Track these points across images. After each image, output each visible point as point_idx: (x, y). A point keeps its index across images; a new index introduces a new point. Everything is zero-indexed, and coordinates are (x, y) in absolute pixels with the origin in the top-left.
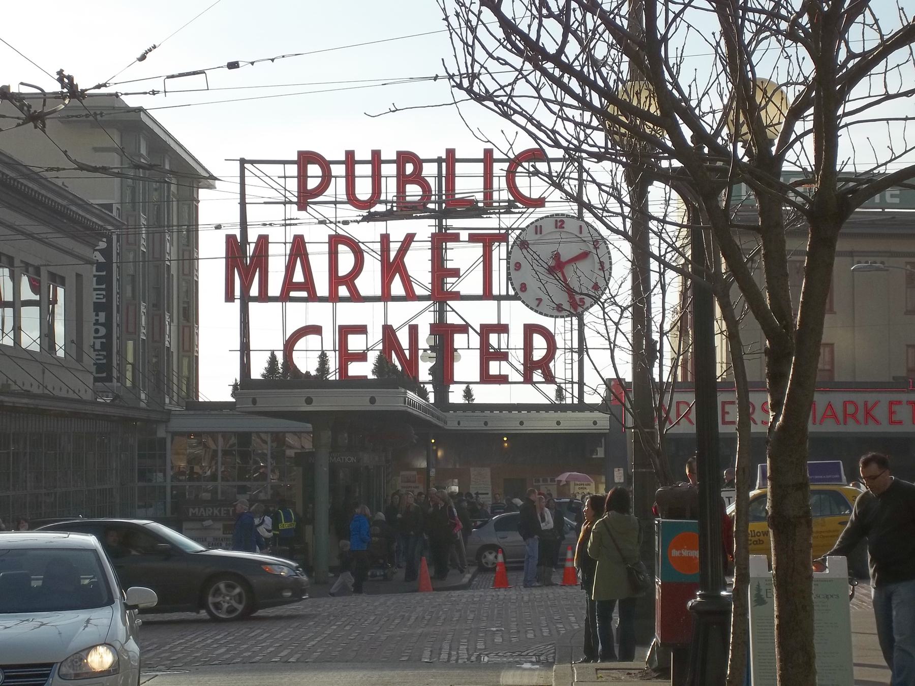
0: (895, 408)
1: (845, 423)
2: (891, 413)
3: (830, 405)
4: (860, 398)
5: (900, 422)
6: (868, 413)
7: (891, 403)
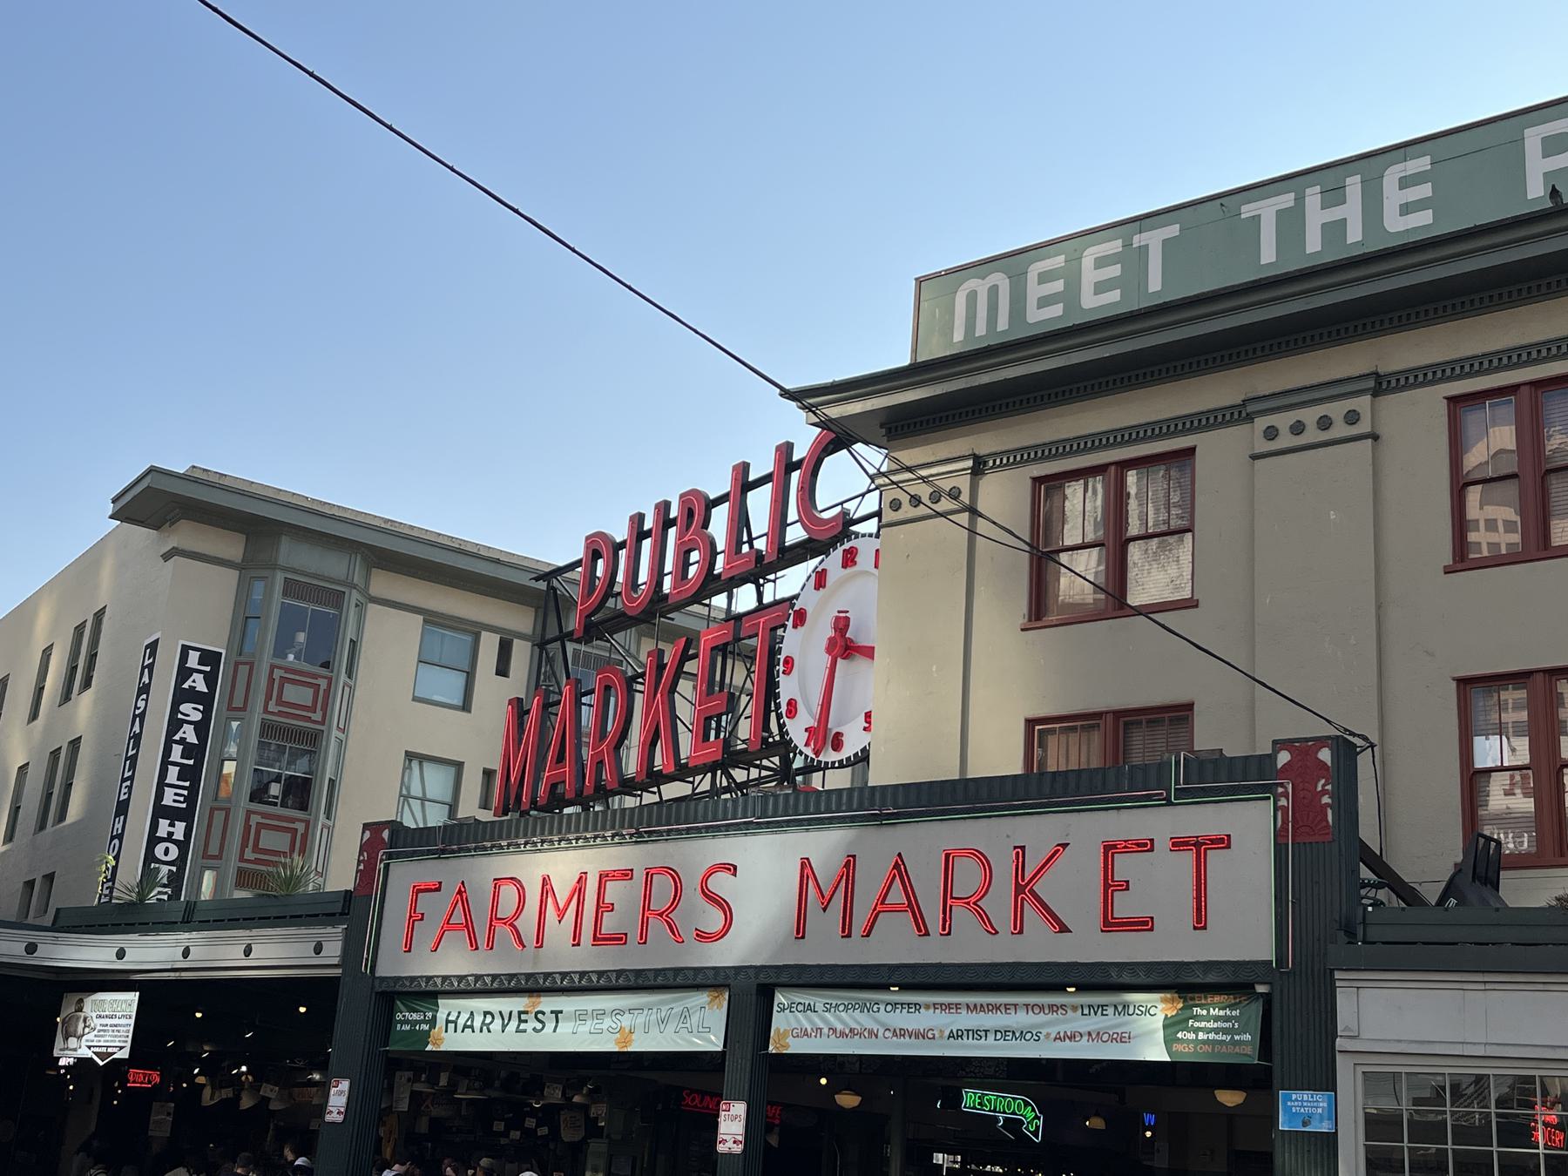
0: (1124, 866)
1: (947, 930)
2: (1111, 886)
3: (899, 868)
4: (996, 836)
5: (1144, 925)
6: (1022, 889)
7: (1110, 849)
